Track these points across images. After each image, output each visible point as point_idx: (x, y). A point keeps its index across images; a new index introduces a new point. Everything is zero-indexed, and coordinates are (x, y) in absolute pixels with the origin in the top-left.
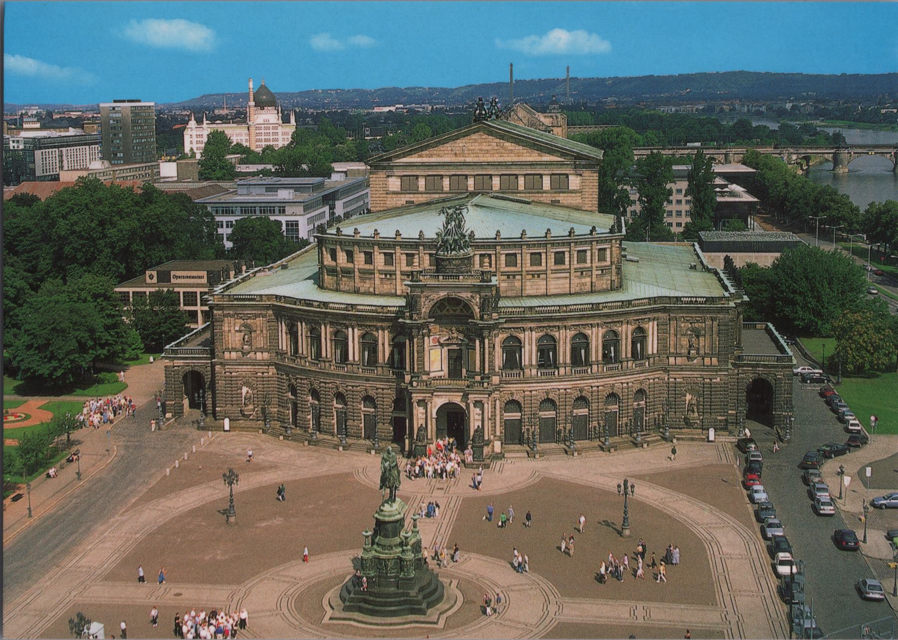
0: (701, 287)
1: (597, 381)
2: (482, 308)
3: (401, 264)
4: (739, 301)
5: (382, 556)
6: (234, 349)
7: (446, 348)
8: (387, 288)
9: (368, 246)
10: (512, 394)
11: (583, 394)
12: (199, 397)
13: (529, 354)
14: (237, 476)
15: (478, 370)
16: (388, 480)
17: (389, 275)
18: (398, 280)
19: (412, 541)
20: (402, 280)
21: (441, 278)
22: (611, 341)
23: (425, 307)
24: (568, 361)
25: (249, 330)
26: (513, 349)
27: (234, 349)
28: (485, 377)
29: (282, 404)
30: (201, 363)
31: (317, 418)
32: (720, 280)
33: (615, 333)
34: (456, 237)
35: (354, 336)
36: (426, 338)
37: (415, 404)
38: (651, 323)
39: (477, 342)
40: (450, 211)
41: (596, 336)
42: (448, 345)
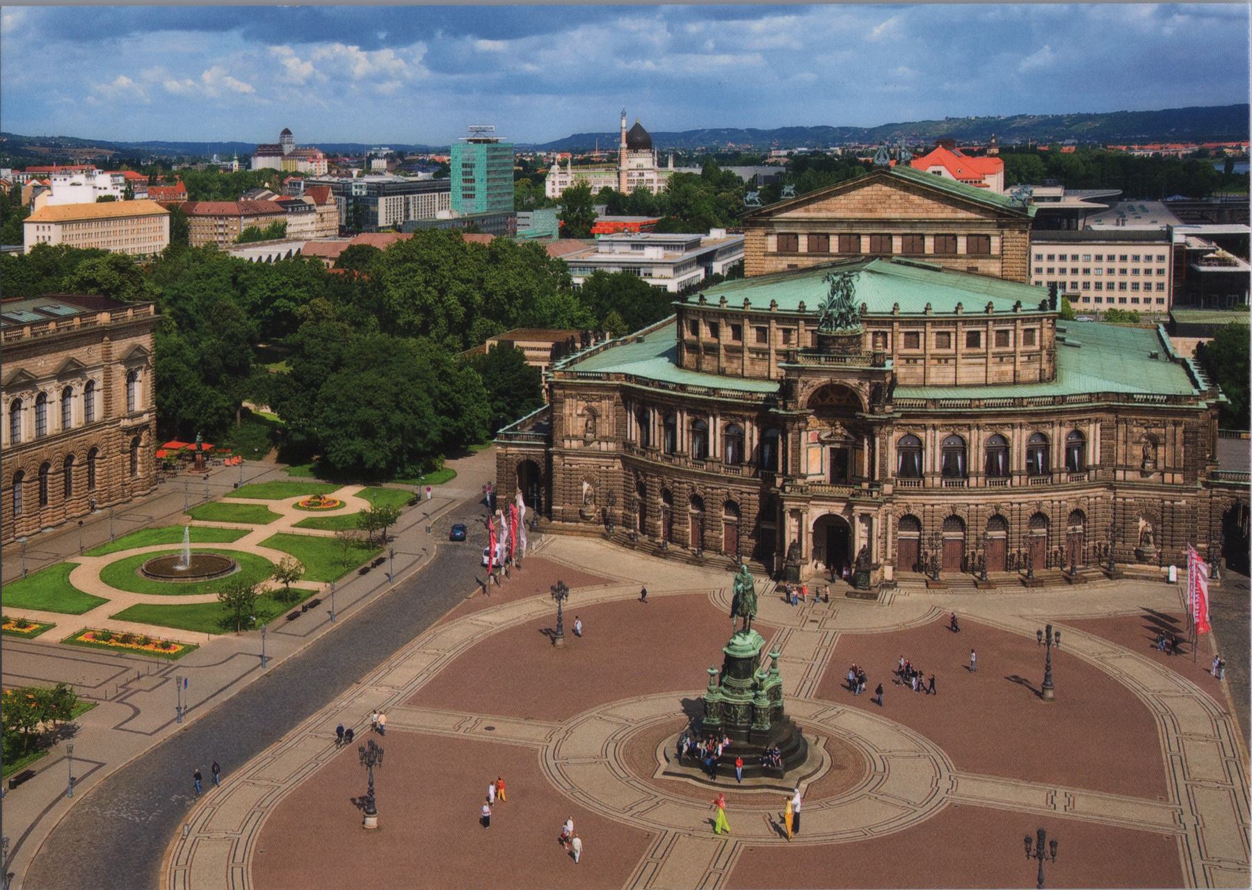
0: (1166, 381)
1: (1019, 499)
2: (875, 396)
4: (1213, 401)
5: (731, 701)
6: (575, 437)
7: (828, 447)
9: (736, 319)
10: (908, 507)
11: (1000, 512)
12: (533, 492)
13: (933, 459)
14: (567, 590)
15: (866, 475)
16: (742, 606)
17: (763, 354)
18: (773, 361)
19: (769, 684)
20: (778, 361)
21: (823, 359)
22: (1041, 445)
24: (981, 469)
25: (594, 414)
26: (911, 453)
27: (575, 437)
28: (874, 484)
29: (628, 505)
31: (669, 524)
32: (1190, 374)
33: (1044, 437)
34: (843, 310)
35: (716, 426)
36: (804, 434)
37: (787, 515)
38: (1092, 426)
39: (866, 442)
40: (837, 279)
41: (1019, 439)
42: (830, 443)
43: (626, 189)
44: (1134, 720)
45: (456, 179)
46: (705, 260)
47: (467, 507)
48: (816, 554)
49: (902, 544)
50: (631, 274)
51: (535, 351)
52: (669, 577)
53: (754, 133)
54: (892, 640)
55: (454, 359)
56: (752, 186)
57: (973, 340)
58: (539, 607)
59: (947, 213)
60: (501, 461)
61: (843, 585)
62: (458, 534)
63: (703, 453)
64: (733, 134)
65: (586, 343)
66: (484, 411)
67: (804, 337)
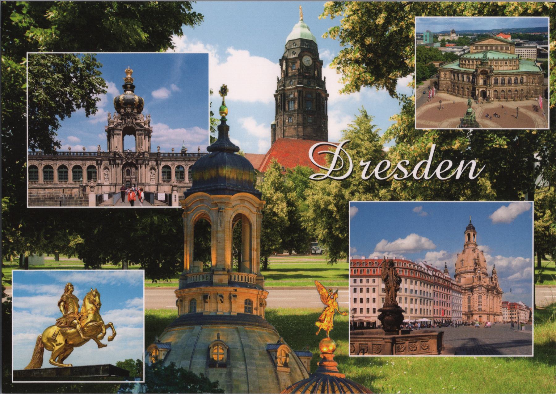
0: (536, 69)
2: (490, 72)
9: (469, 60)
13: (499, 81)
17: (473, 65)
23: (479, 71)
25: (445, 74)
26: (496, 81)
28: (490, 85)
29: (451, 88)
30: (437, 80)
35: (465, 76)
41: (513, 78)
43: (451, 40)
45: (424, 38)
46: (464, 50)
47: (426, 88)
49: (495, 95)
50: (452, 52)
51: (437, 64)
52: (458, 100)
55: (424, 66)
56: (471, 39)
57: (506, 63)
58: (437, 104)
59: (502, 43)
62: (424, 93)
63: (463, 81)
64: (469, 31)
66: (428, 74)
67: (479, 63)
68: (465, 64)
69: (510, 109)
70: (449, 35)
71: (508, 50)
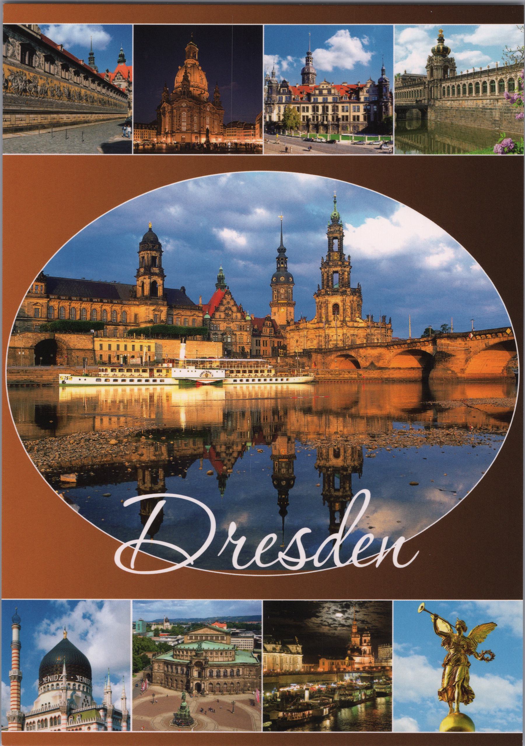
1: (229, 680)
2: (205, 663)
3: (189, 654)
8: (187, 658)
9: (183, 650)
13: (215, 674)
17: (187, 656)
22: (232, 671)
23: (193, 663)
25: (159, 666)
26: (211, 672)
28: (205, 678)
29: (165, 681)
30: (150, 672)
35: (179, 668)
41: (229, 670)
43: (165, 629)
44: (248, 717)
46: (178, 640)
47: (138, 681)
48: (196, 689)
50: (166, 643)
51: (150, 655)
53: (186, 619)
54: (208, 703)
56: (185, 628)
57: (221, 654)
58: (149, 698)
59: (217, 633)
60: (144, 673)
61: (200, 695)
63: (177, 673)
65: (158, 654)
67: (194, 653)
68: (179, 655)
69: (224, 703)
70: (162, 624)
71: (224, 640)
